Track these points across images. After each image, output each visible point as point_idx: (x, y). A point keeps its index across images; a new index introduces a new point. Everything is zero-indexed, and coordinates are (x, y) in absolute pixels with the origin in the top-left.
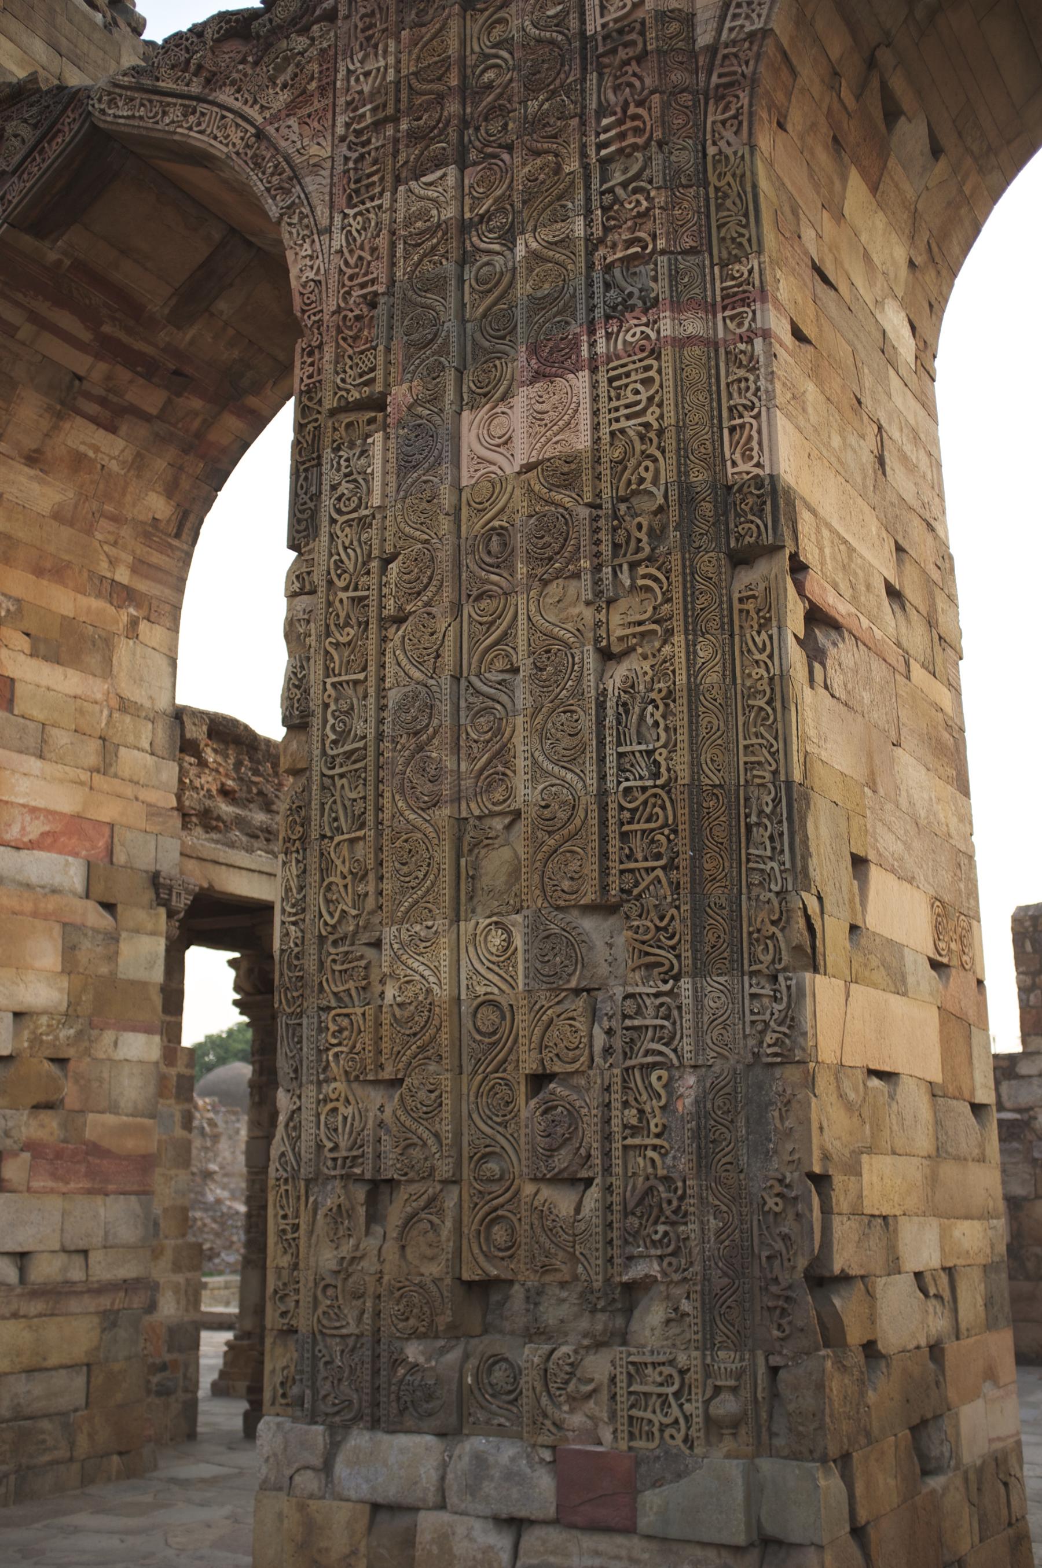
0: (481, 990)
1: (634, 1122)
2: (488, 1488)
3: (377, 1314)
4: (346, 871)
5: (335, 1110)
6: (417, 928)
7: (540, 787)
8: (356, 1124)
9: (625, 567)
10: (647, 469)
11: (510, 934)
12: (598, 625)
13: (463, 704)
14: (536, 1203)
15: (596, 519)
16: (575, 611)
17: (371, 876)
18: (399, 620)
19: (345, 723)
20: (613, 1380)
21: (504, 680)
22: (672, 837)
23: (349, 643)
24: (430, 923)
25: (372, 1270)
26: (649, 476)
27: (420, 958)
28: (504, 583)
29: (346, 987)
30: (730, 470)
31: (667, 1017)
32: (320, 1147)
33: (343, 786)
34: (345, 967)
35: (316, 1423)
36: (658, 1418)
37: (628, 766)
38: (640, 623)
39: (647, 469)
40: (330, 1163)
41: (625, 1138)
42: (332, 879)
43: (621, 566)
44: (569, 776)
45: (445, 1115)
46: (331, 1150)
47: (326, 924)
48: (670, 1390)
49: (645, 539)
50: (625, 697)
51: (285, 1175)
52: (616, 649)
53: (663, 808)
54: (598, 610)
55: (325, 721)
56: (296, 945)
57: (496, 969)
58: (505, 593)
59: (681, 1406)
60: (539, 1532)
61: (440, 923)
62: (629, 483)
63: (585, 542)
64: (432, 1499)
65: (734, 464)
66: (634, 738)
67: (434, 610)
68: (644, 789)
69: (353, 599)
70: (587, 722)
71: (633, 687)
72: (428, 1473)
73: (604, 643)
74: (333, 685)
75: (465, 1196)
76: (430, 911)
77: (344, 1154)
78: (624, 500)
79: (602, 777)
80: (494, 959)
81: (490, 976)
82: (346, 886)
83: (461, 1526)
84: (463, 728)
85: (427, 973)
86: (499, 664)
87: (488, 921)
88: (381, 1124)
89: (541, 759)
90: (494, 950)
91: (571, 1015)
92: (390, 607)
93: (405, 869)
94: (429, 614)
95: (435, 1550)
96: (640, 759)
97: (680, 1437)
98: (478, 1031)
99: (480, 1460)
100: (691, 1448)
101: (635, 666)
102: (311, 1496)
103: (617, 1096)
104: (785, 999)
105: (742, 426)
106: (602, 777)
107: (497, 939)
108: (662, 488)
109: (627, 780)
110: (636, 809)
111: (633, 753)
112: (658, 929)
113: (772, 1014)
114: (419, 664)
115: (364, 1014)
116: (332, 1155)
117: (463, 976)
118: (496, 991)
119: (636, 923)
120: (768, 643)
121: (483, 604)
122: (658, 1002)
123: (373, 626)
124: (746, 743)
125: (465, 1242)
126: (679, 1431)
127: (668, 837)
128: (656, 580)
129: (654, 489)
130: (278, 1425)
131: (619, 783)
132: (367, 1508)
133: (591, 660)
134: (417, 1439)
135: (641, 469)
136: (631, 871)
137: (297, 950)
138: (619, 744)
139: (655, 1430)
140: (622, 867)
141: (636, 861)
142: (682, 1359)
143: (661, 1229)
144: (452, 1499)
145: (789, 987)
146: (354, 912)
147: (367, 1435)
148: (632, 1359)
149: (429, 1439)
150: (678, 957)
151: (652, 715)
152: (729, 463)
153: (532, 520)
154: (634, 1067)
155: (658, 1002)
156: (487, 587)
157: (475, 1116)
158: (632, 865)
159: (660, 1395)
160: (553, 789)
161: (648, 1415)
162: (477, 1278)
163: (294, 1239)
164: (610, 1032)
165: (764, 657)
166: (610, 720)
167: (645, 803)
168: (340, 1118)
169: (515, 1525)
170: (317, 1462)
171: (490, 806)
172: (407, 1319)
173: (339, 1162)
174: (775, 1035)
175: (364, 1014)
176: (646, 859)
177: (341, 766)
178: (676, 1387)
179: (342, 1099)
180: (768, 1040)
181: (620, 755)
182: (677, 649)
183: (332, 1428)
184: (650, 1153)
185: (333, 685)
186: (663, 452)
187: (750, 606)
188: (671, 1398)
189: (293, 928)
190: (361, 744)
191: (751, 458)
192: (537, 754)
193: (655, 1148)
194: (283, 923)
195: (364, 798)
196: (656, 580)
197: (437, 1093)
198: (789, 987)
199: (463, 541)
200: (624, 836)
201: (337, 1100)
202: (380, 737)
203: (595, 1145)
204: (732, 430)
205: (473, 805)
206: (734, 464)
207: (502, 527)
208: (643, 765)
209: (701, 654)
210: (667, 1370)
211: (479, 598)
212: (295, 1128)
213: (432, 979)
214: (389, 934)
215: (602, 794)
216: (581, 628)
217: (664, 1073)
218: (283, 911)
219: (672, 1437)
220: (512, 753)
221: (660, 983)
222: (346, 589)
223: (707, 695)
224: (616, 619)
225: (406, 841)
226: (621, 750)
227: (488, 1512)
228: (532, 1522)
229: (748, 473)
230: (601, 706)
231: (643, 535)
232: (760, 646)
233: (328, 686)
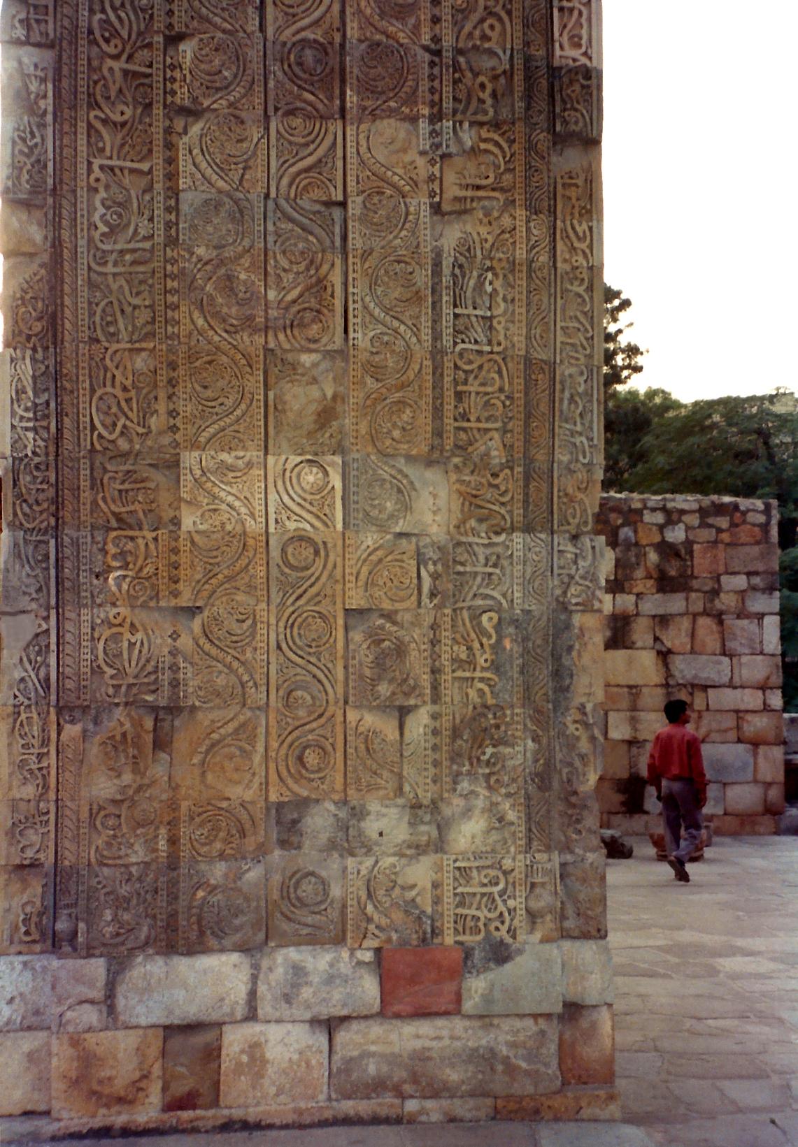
0: (291, 525)
1: (463, 656)
2: (306, 993)
3: (173, 841)
4: (128, 383)
5: (116, 637)
6: (224, 456)
7: (372, 334)
8: (145, 650)
9: (466, 125)
10: (492, 27)
11: (326, 473)
12: (431, 179)
13: (270, 228)
14: (361, 729)
15: (432, 64)
16: (407, 158)
17: (162, 395)
18: (192, 113)
19: (120, 216)
20: (436, 885)
21: (319, 212)
22: (508, 403)
23: (123, 124)
24: (241, 454)
25: (164, 797)
26: (494, 35)
27: (228, 488)
28: (320, 106)
29: (131, 508)
30: (558, 52)
31: (495, 566)
32: (97, 671)
33: (121, 287)
34: (126, 486)
35: (93, 956)
36: (483, 914)
37: (462, 328)
38: (478, 188)
39: (492, 27)
40: (111, 691)
41: (453, 671)
42: (109, 389)
43: (461, 123)
44: (403, 328)
45: (260, 645)
46: (112, 677)
47: (100, 436)
48: (496, 890)
49: (489, 101)
50: (462, 260)
51: (27, 702)
52: (446, 207)
53: (500, 372)
54: (432, 162)
55: (91, 209)
56: (34, 453)
57: (307, 505)
58: (321, 117)
59: (505, 901)
60: (355, 1026)
61: (254, 454)
62: (470, 35)
63: (424, 86)
64: (240, 1013)
65: (562, 47)
66: (469, 302)
67: (243, 115)
68: (480, 352)
69: (126, 73)
70: (422, 278)
71: (469, 250)
72: (237, 987)
73: (437, 199)
74: (102, 167)
75: (272, 722)
76: (240, 441)
77: (132, 681)
78: (460, 52)
79: (437, 337)
80: (309, 497)
81: (304, 514)
82: (128, 401)
83: (274, 1033)
84: (270, 254)
85: (237, 504)
86: (316, 194)
87: (299, 459)
88: (174, 653)
89: (372, 305)
90: (308, 487)
91: (399, 557)
92: (182, 96)
93: (209, 393)
94: (236, 117)
95: (245, 1058)
96: (475, 325)
97: (504, 928)
98: (291, 567)
99: (298, 971)
100: (514, 937)
101: (469, 228)
102: (90, 1029)
103: (447, 634)
104: (590, 557)
105: (571, 10)
106: (437, 337)
107: (311, 477)
108: (508, 52)
109: (463, 342)
110: (472, 371)
111: (468, 316)
112: (490, 485)
113: (577, 569)
114: (222, 170)
115: (156, 539)
116: (115, 682)
117: (271, 510)
118: (308, 527)
119: (467, 478)
120: (588, 233)
121: (297, 122)
122: (488, 551)
123: (158, 110)
124: (563, 324)
125: (272, 766)
126: (503, 923)
127: (503, 403)
128: (497, 144)
129: (501, 54)
130: (25, 964)
131: (455, 344)
132: (161, 1032)
133: (425, 212)
134: (224, 958)
135: (486, 25)
136: (464, 429)
137: (37, 460)
138: (455, 306)
139: (481, 924)
140: (457, 424)
141: (468, 420)
142: (507, 863)
143: (489, 751)
144: (265, 1009)
145: (593, 548)
146: (141, 430)
147: (160, 961)
148: (458, 864)
149: (235, 957)
150: (510, 512)
151: (491, 283)
152: (557, 45)
153: (363, 46)
154: (462, 608)
155: (488, 551)
156: (299, 104)
157: (284, 646)
158: (466, 424)
159: (483, 895)
160: (386, 338)
161: (473, 912)
162: (287, 799)
163: (40, 769)
164: (435, 576)
165: (584, 246)
166: (446, 279)
167: (480, 367)
168: (126, 644)
169: (330, 1025)
170: (98, 994)
171: (303, 343)
172: (210, 843)
173: (123, 689)
174: (579, 588)
175: (156, 539)
176: (478, 420)
177: (115, 264)
178: (501, 886)
179: (127, 625)
180: (572, 590)
181: (456, 316)
182: (518, 223)
183: (111, 959)
184: (481, 685)
185: (102, 167)
186: (509, 13)
187: (573, 193)
188: (497, 897)
189: (30, 435)
190: (147, 245)
191: (580, 46)
192: (368, 299)
193: (482, 680)
194: (13, 427)
195: (151, 306)
196: (497, 144)
197: (249, 622)
198: (593, 548)
199: (269, 44)
200: (459, 396)
201: (120, 625)
202: (172, 242)
203: (425, 677)
204: (561, 9)
205: (281, 336)
206: (562, 47)
207: (315, 41)
208: (479, 330)
209: (535, 232)
210: (493, 873)
211: (291, 113)
212: (39, 653)
213: (243, 510)
214: (190, 459)
215: (437, 353)
216: (415, 177)
217: (495, 616)
218: (13, 414)
219: (497, 929)
220: (329, 290)
221: (492, 535)
222: (116, 57)
223: (539, 273)
224: (450, 178)
225: (210, 363)
226: (458, 311)
227: (308, 1016)
228: (345, 1019)
229: (574, 60)
230: (437, 264)
231: (486, 95)
232: (581, 234)
233: (96, 168)
